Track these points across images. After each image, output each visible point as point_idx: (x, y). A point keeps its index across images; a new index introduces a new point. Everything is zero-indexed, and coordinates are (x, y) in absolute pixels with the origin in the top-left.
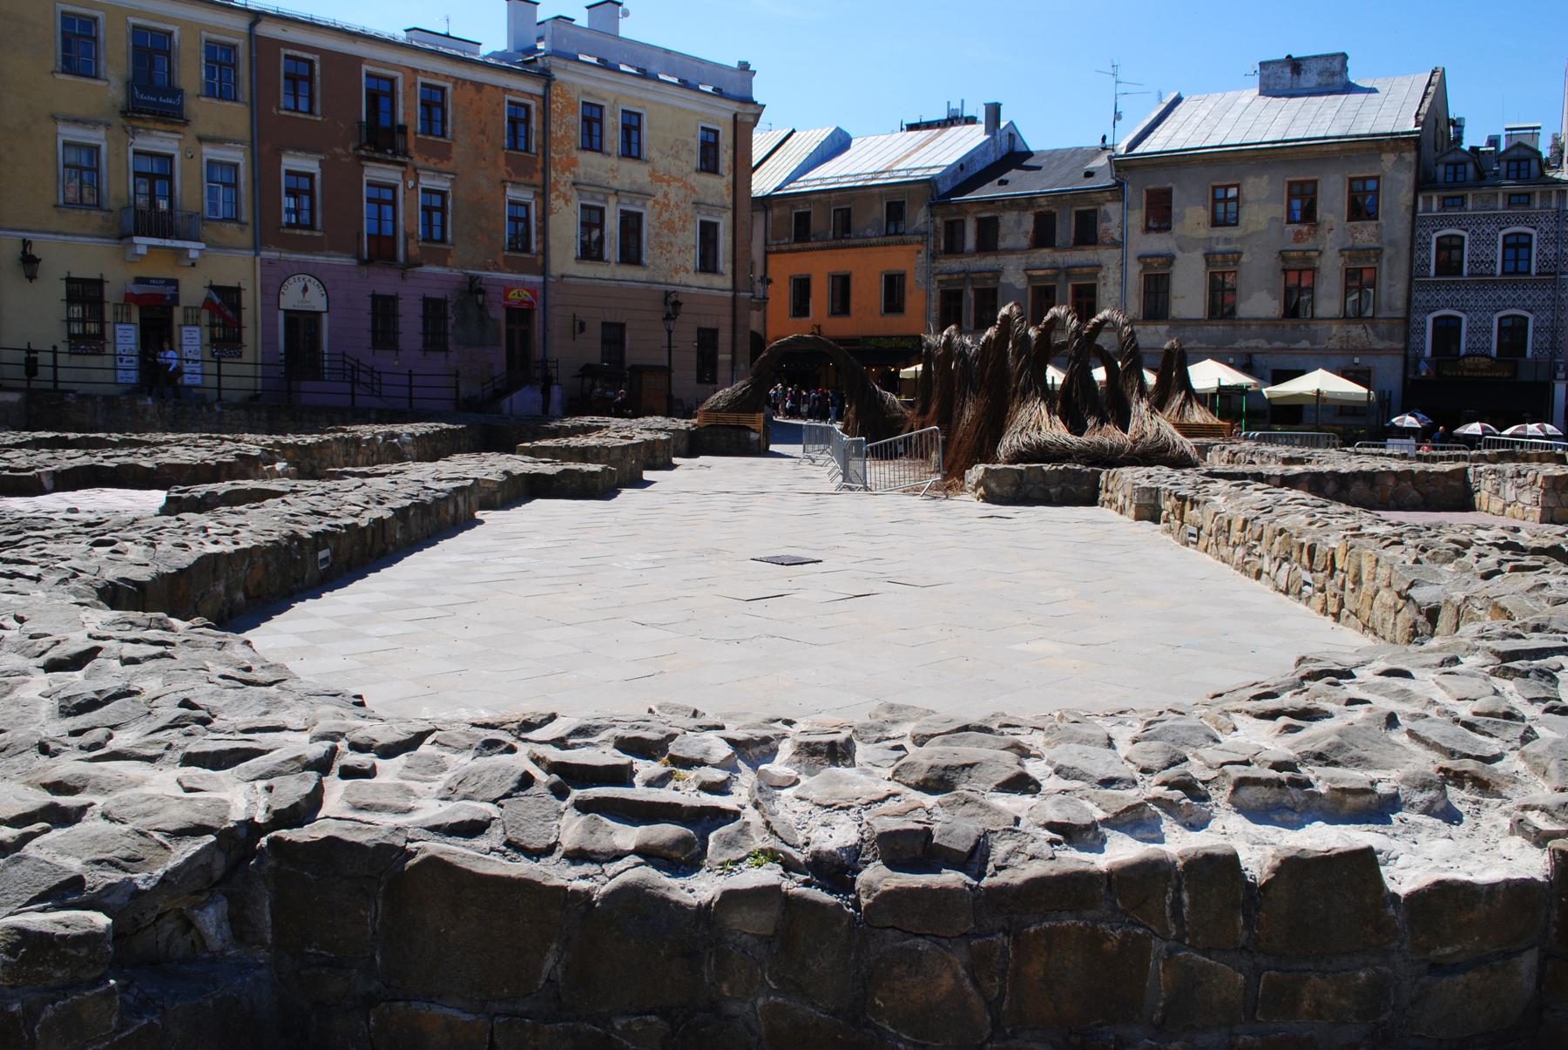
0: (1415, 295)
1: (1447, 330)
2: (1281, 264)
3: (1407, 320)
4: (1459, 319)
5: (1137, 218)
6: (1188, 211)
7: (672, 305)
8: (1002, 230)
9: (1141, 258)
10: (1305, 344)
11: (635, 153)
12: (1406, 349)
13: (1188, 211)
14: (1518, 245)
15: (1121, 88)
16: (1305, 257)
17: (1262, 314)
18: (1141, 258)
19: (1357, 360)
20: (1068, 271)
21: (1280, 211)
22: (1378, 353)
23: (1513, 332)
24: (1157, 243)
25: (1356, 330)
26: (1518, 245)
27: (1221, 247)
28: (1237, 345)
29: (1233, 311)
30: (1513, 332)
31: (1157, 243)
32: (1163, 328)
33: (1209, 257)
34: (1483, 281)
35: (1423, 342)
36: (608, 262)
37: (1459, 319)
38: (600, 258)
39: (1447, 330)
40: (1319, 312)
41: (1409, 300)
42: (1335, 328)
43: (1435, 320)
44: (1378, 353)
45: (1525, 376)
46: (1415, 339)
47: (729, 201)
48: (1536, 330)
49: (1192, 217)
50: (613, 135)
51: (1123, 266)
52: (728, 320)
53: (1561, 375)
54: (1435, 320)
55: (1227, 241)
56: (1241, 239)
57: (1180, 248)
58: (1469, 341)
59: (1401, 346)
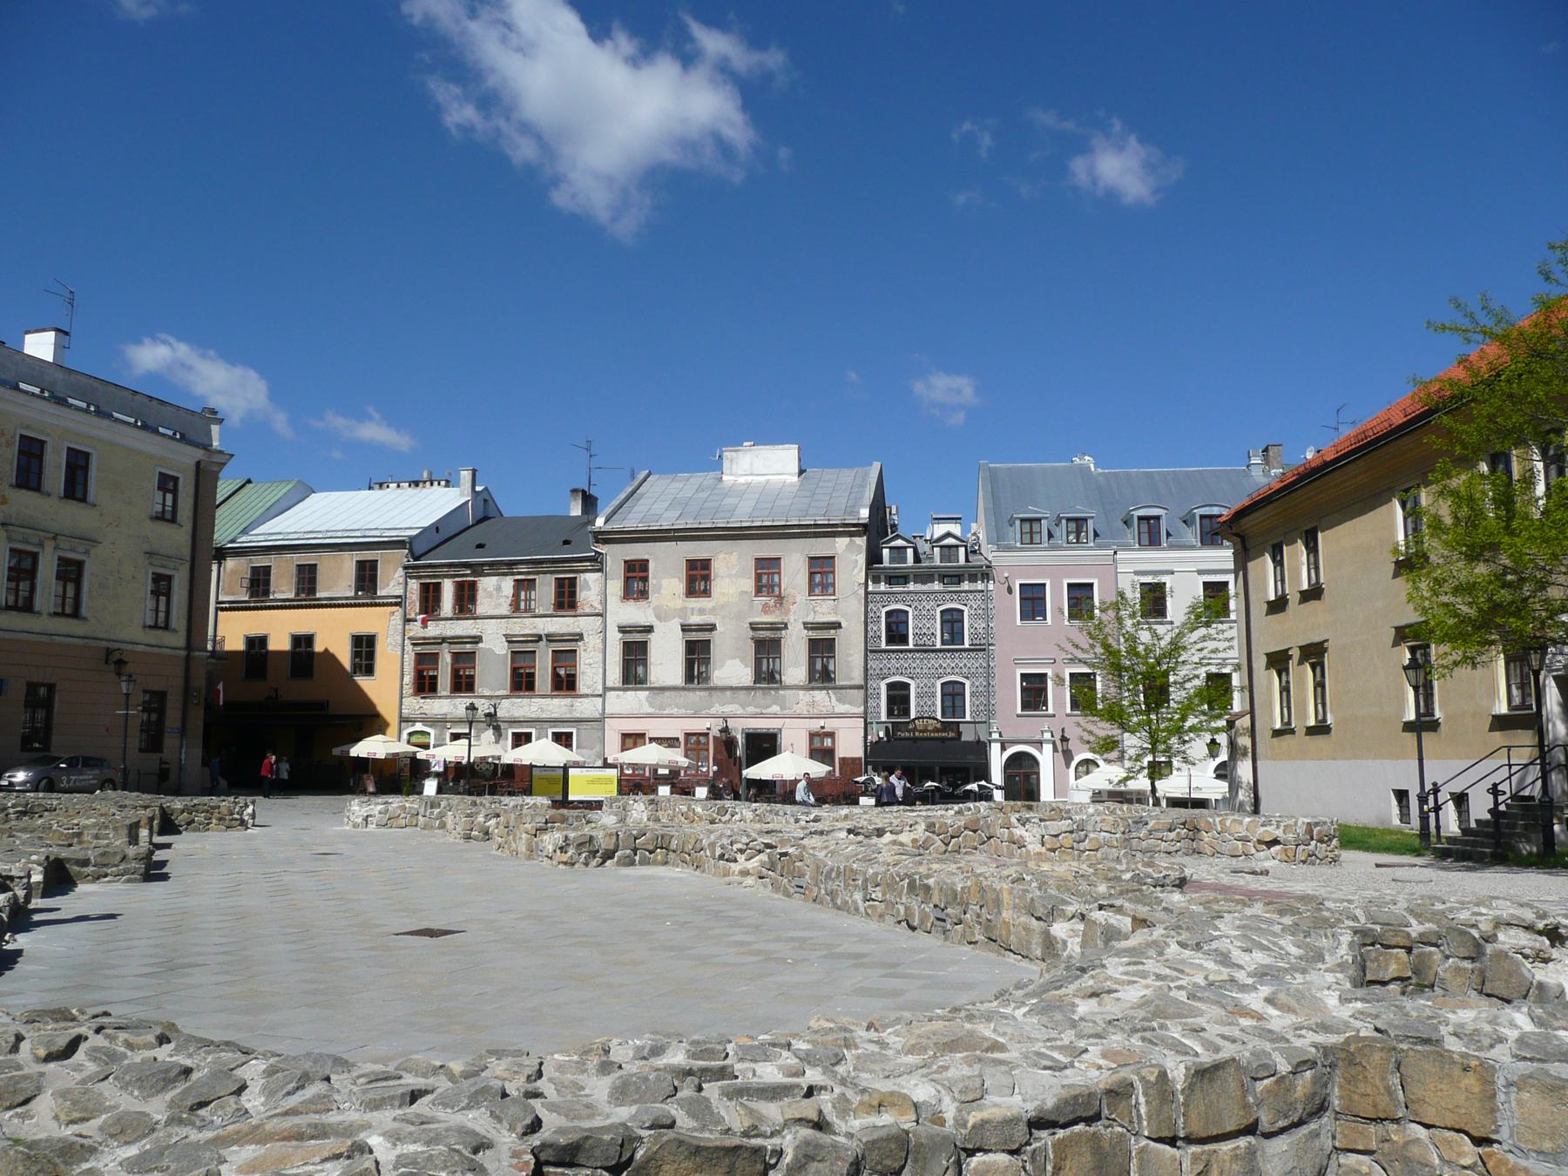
0: (870, 663)
1: (898, 697)
2: (751, 633)
4: (908, 685)
5: (616, 586)
6: (664, 582)
7: (115, 660)
8: (480, 595)
9: (623, 630)
10: (775, 709)
11: (79, 495)
12: (866, 712)
13: (664, 582)
14: (952, 621)
15: (595, 462)
16: (774, 627)
18: (623, 630)
20: (551, 638)
21: (749, 584)
23: (953, 694)
24: (635, 613)
25: (820, 696)
26: (952, 621)
27: (695, 619)
28: (713, 711)
29: (708, 679)
30: (953, 694)
31: (635, 613)
32: (643, 695)
33: (685, 629)
35: (878, 706)
36: (39, 613)
37: (908, 685)
38: (27, 607)
39: (898, 697)
45: (968, 736)
46: (871, 703)
47: (186, 552)
49: (668, 584)
50: (54, 474)
51: (604, 631)
52: (180, 682)
54: (891, 686)
55: (701, 611)
56: (713, 611)
57: (658, 617)
58: (918, 705)
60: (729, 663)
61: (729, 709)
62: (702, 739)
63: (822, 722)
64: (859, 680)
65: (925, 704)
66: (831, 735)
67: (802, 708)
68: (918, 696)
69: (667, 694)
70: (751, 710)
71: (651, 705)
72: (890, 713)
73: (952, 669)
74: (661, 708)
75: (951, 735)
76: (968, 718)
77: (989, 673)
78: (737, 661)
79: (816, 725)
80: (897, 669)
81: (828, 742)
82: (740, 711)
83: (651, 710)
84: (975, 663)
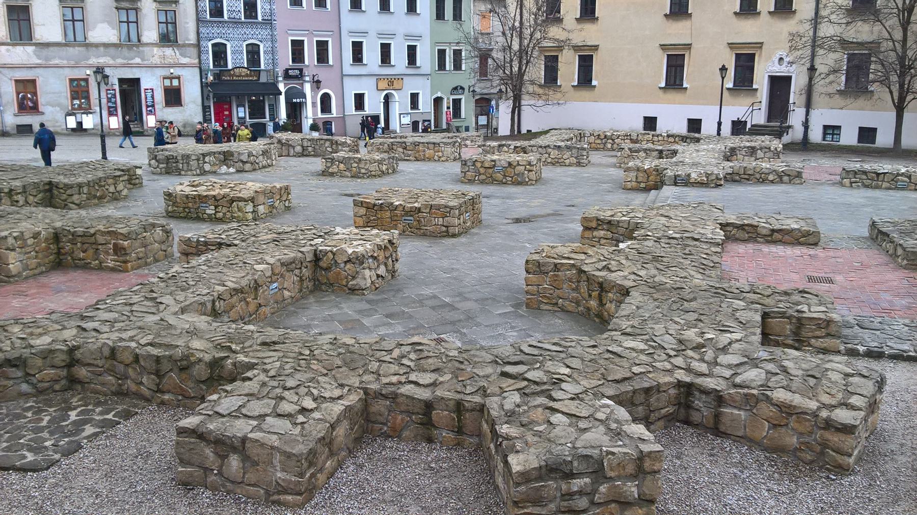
3: (198, 46)
10: (138, 60)
17: (105, 40)
19: (172, 71)
22: (184, 66)
23: (253, 52)
25: (169, 51)
28: (90, 62)
30: (253, 52)
32: (30, 49)
34: (235, 23)
35: (208, 58)
37: (225, 45)
39: (220, 53)
40: (144, 39)
41: (198, 33)
42: (155, 49)
43: (213, 45)
44: (184, 66)
45: (263, 79)
46: (203, 57)
48: (265, 52)
53: (280, 79)
54: (213, 45)
58: (233, 58)
59: (197, 61)
60: (100, 25)
61: (102, 61)
62: (83, 83)
63: (172, 71)
64: (192, 39)
65: (236, 59)
66: (178, 78)
67: (156, 60)
68: (233, 53)
69: (51, 49)
70: (120, 61)
71: (39, 57)
72: (214, 65)
73: (255, 36)
74: (47, 59)
75: (255, 78)
76: (263, 67)
77: (273, 40)
78: (105, 25)
79: (165, 72)
80: (216, 35)
81: (175, 83)
82: (111, 62)
83: (39, 61)
84: (265, 33)
